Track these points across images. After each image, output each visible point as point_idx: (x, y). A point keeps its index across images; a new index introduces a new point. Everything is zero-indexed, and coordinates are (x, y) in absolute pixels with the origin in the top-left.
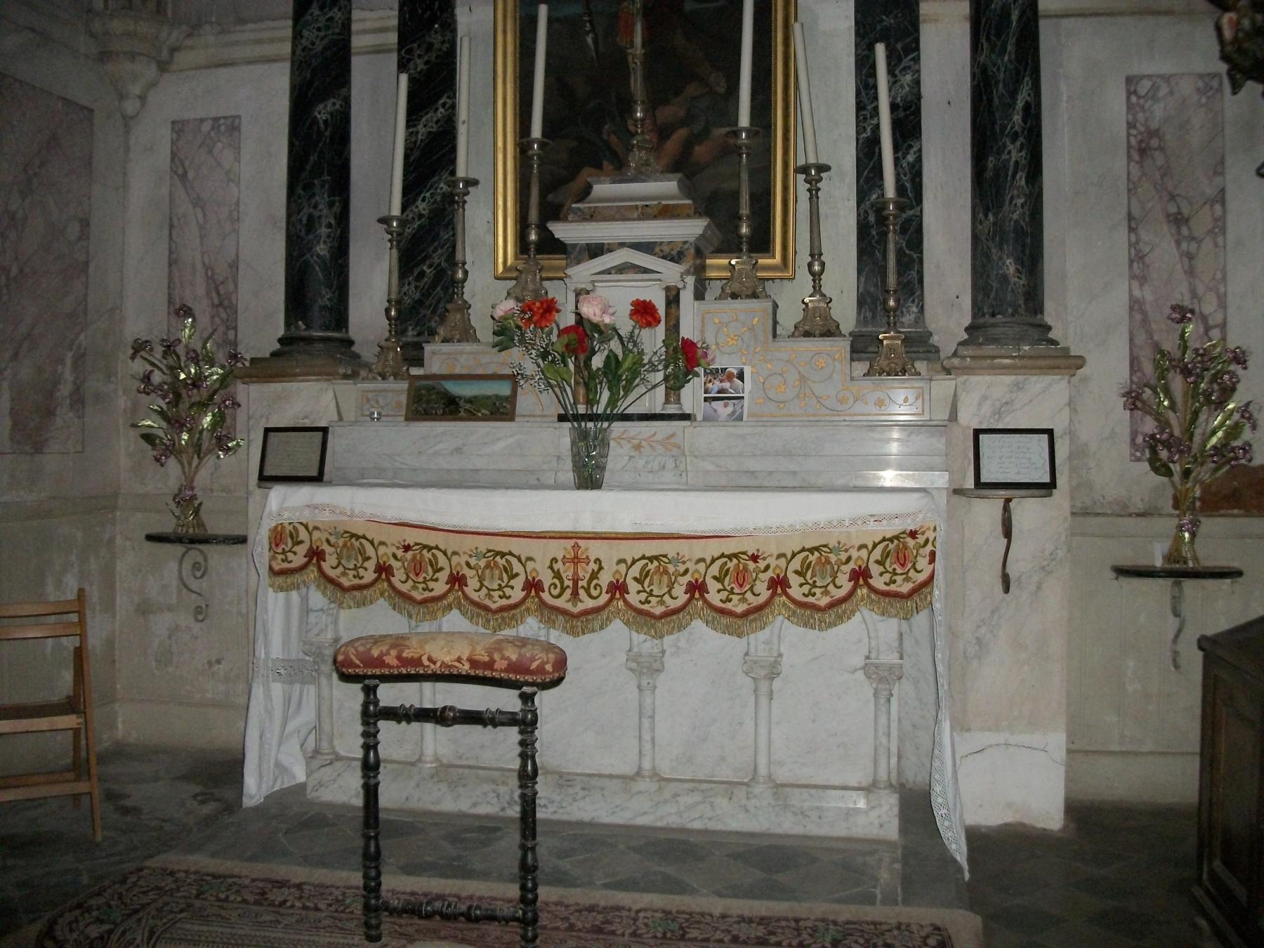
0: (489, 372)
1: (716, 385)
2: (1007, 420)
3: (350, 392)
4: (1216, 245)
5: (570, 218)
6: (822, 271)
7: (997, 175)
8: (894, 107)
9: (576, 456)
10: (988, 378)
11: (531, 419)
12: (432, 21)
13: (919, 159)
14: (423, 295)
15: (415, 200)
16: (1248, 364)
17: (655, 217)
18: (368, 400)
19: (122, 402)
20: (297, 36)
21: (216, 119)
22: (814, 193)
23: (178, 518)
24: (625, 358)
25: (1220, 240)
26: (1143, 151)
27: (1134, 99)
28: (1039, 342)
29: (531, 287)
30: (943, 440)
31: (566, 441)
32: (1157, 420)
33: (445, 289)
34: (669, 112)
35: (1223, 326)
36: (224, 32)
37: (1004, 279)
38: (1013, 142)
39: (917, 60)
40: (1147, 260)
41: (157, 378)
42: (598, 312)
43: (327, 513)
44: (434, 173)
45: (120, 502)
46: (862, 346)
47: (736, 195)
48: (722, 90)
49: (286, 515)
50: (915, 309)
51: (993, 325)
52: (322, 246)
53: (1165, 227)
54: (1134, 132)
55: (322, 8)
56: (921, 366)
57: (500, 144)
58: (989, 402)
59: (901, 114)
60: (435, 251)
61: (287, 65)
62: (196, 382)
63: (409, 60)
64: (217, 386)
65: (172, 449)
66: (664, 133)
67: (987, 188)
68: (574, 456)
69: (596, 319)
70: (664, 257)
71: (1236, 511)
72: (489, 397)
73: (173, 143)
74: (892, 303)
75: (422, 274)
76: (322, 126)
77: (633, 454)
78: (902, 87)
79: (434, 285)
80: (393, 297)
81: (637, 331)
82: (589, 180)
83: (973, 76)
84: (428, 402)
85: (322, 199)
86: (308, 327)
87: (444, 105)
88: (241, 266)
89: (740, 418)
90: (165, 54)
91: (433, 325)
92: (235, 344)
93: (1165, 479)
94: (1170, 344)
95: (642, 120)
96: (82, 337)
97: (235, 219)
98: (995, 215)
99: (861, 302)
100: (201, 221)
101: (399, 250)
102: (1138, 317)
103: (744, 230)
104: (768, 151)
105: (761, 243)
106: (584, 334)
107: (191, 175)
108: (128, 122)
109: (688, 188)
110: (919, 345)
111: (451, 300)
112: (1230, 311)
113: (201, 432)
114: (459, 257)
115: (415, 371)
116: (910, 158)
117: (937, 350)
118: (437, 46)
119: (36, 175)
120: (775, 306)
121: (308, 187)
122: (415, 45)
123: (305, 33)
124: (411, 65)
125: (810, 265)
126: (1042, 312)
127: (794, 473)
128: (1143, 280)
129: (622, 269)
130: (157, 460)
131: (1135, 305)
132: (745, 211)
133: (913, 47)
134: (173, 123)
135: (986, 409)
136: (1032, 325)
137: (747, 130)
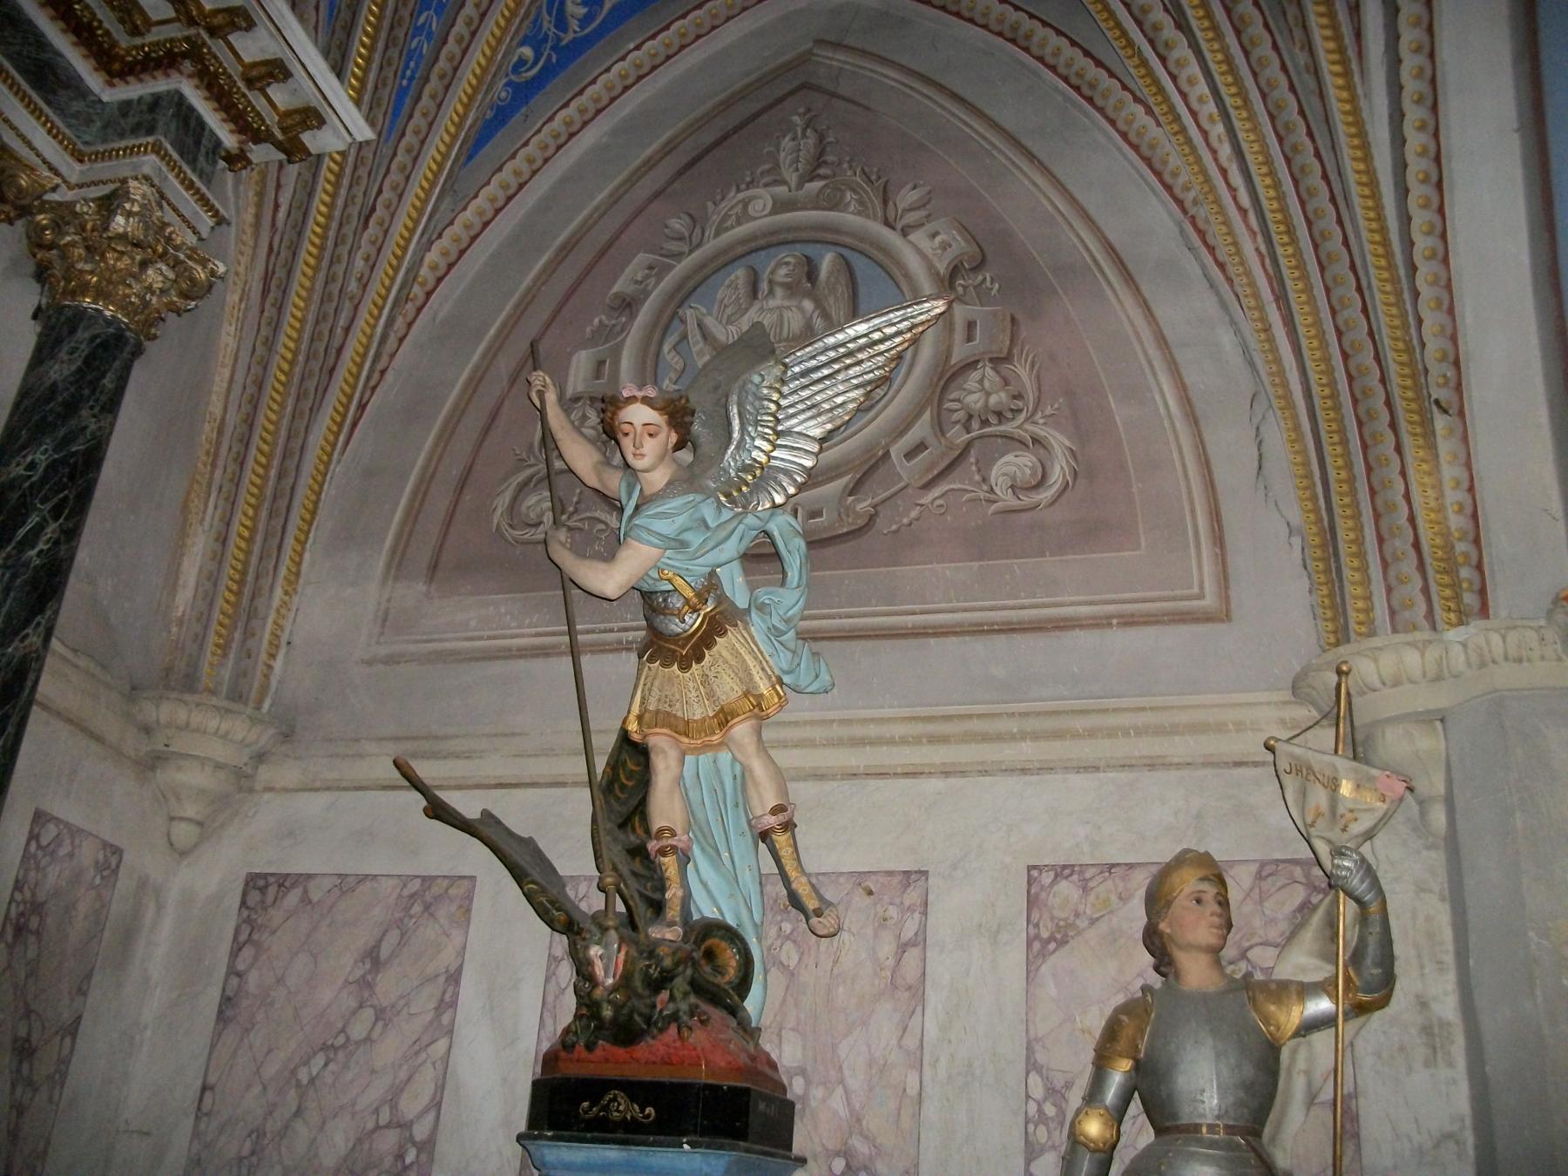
54: (18, 896)
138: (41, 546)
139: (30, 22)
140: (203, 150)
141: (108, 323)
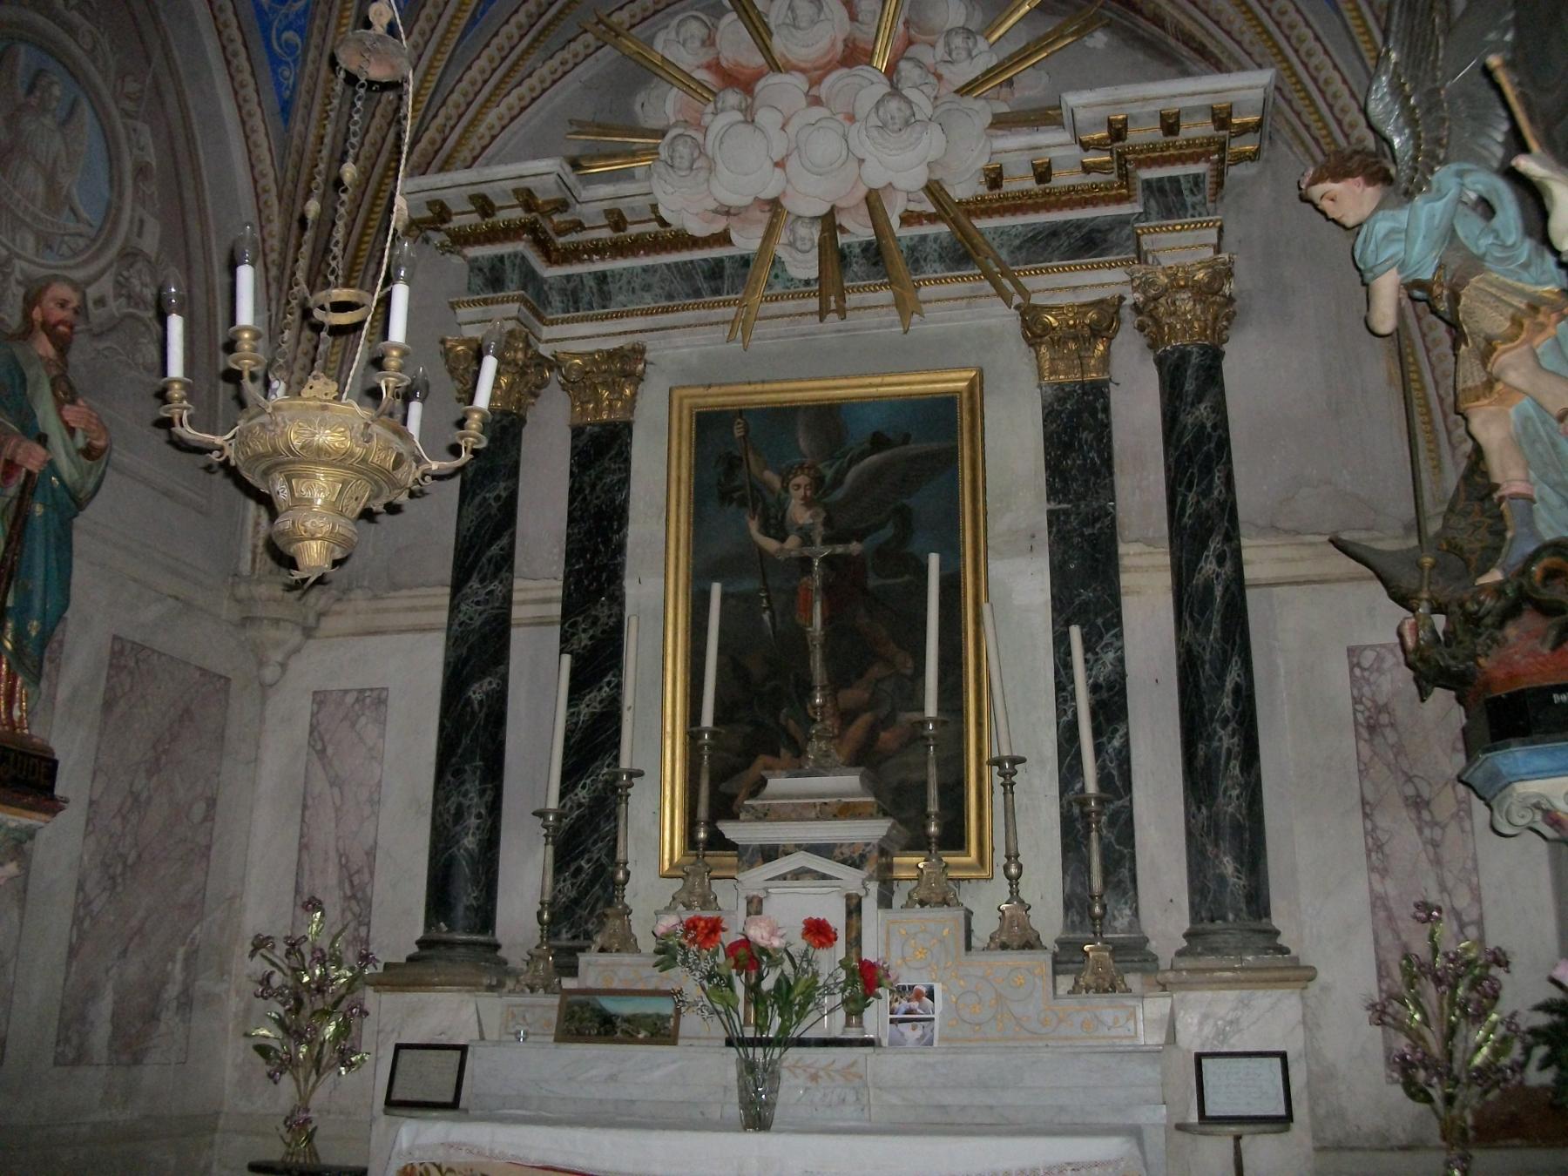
0: (651, 987)
1: (903, 1005)
2: (1232, 1041)
3: (493, 1006)
4: (1463, 831)
5: (742, 816)
6: (1019, 875)
7: (1208, 761)
8: (1094, 688)
9: (743, 1089)
10: (1208, 994)
11: (696, 1042)
12: (600, 592)
13: (1126, 744)
14: (579, 893)
15: (575, 786)
16: (1511, 967)
17: (835, 817)
18: (514, 1016)
19: (234, 1004)
20: (454, 609)
21: (362, 691)
22: (1008, 787)
23: (289, 1145)
24: (797, 980)
25: (1467, 826)
26: (1372, 729)
27: (1357, 671)
28: (1265, 951)
29: (698, 890)
30: (1159, 1069)
31: (733, 1073)
32: (1408, 1036)
33: (605, 888)
34: (852, 696)
35: (1480, 923)
36: (376, 597)
37: (1222, 879)
38: (1224, 728)
39: (1119, 636)
40: (1387, 849)
41: (277, 980)
42: (765, 935)
43: (463, 1153)
44: (595, 759)
45: (221, 1122)
46: (1067, 958)
47: (924, 785)
48: (909, 672)
49: (417, 1154)
50: (1127, 912)
51: (1214, 933)
52: (470, 838)
53: (1404, 813)
55: (482, 581)
56: (1133, 980)
57: (669, 728)
58: (1211, 1022)
59: (1105, 695)
60: (595, 842)
61: (443, 636)
62: (321, 987)
63: (573, 634)
64: (343, 991)
65: (289, 1064)
66: (847, 717)
67: (1199, 778)
68: (741, 1091)
69: (763, 943)
70: (844, 862)
71: (1517, 1141)
72: (648, 1016)
73: (313, 715)
74: (1097, 910)
75: (579, 870)
76: (476, 706)
77: (809, 1084)
78: (1104, 664)
79: (592, 883)
80: (547, 898)
81: (811, 950)
82: (764, 773)
83: (1179, 656)
84: (581, 1020)
85: (472, 787)
86: (451, 929)
87: (609, 683)
88: (379, 855)
89: (930, 1043)
90: (311, 620)
91: (590, 927)
92: (366, 942)
93: (1427, 1106)
94: (1420, 948)
95: (822, 706)
96: (196, 930)
97: (375, 802)
98: (1209, 808)
99: (1068, 905)
100: (338, 803)
101: (553, 843)
102: (1382, 914)
103: (933, 829)
104: (961, 736)
105: (954, 839)
106: (749, 956)
107: (330, 751)
108: (265, 688)
109: (873, 783)
110: (1133, 953)
111: (609, 903)
112: (1487, 903)
113: (322, 1044)
114: (620, 856)
115: (568, 983)
116: (1116, 743)
117: (1155, 959)
118: (603, 620)
119: (165, 751)
120: (969, 914)
121: (458, 773)
122: (580, 619)
123: (463, 607)
124: (575, 640)
125: (1006, 868)
126: (1268, 915)
127: (991, 1107)
128: (1384, 872)
129: (798, 874)
130: (271, 1076)
131: (1378, 902)
132: (933, 807)
133: (1116, 621)
134: (315, 693)
135: (1208, 1030)
136: (1254, 931)
137: (935, 722)
138: (1189, 511)
139: (1066, 222)
140: (1186, 193)
141: (1172, 353)
